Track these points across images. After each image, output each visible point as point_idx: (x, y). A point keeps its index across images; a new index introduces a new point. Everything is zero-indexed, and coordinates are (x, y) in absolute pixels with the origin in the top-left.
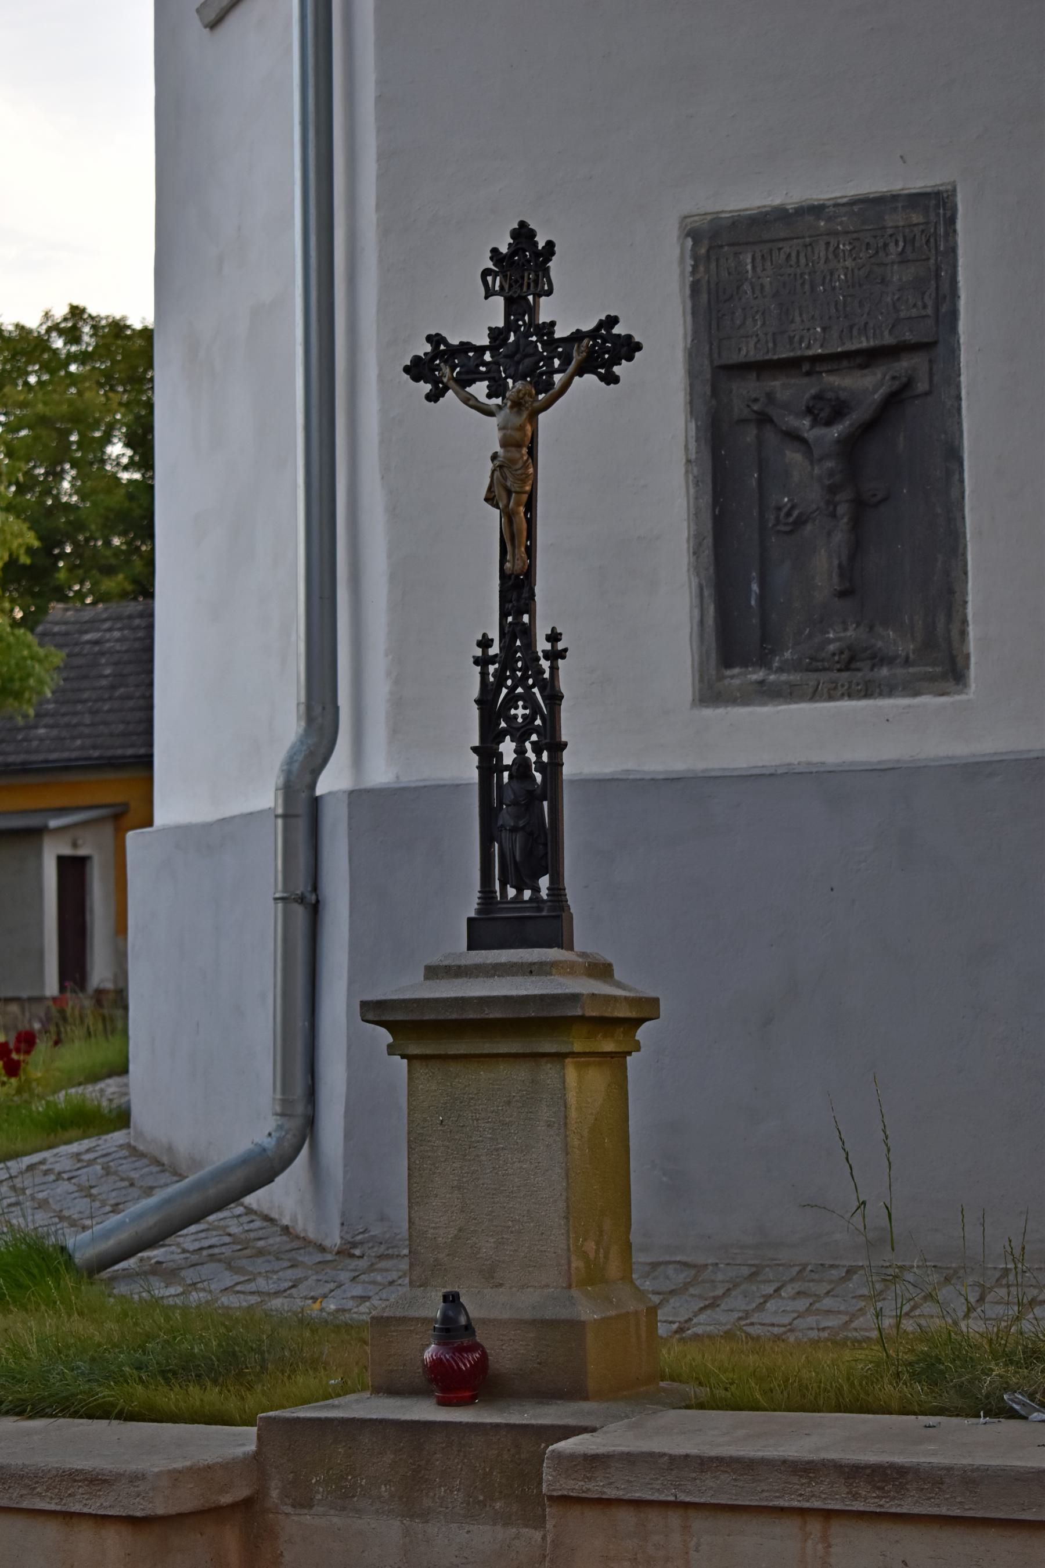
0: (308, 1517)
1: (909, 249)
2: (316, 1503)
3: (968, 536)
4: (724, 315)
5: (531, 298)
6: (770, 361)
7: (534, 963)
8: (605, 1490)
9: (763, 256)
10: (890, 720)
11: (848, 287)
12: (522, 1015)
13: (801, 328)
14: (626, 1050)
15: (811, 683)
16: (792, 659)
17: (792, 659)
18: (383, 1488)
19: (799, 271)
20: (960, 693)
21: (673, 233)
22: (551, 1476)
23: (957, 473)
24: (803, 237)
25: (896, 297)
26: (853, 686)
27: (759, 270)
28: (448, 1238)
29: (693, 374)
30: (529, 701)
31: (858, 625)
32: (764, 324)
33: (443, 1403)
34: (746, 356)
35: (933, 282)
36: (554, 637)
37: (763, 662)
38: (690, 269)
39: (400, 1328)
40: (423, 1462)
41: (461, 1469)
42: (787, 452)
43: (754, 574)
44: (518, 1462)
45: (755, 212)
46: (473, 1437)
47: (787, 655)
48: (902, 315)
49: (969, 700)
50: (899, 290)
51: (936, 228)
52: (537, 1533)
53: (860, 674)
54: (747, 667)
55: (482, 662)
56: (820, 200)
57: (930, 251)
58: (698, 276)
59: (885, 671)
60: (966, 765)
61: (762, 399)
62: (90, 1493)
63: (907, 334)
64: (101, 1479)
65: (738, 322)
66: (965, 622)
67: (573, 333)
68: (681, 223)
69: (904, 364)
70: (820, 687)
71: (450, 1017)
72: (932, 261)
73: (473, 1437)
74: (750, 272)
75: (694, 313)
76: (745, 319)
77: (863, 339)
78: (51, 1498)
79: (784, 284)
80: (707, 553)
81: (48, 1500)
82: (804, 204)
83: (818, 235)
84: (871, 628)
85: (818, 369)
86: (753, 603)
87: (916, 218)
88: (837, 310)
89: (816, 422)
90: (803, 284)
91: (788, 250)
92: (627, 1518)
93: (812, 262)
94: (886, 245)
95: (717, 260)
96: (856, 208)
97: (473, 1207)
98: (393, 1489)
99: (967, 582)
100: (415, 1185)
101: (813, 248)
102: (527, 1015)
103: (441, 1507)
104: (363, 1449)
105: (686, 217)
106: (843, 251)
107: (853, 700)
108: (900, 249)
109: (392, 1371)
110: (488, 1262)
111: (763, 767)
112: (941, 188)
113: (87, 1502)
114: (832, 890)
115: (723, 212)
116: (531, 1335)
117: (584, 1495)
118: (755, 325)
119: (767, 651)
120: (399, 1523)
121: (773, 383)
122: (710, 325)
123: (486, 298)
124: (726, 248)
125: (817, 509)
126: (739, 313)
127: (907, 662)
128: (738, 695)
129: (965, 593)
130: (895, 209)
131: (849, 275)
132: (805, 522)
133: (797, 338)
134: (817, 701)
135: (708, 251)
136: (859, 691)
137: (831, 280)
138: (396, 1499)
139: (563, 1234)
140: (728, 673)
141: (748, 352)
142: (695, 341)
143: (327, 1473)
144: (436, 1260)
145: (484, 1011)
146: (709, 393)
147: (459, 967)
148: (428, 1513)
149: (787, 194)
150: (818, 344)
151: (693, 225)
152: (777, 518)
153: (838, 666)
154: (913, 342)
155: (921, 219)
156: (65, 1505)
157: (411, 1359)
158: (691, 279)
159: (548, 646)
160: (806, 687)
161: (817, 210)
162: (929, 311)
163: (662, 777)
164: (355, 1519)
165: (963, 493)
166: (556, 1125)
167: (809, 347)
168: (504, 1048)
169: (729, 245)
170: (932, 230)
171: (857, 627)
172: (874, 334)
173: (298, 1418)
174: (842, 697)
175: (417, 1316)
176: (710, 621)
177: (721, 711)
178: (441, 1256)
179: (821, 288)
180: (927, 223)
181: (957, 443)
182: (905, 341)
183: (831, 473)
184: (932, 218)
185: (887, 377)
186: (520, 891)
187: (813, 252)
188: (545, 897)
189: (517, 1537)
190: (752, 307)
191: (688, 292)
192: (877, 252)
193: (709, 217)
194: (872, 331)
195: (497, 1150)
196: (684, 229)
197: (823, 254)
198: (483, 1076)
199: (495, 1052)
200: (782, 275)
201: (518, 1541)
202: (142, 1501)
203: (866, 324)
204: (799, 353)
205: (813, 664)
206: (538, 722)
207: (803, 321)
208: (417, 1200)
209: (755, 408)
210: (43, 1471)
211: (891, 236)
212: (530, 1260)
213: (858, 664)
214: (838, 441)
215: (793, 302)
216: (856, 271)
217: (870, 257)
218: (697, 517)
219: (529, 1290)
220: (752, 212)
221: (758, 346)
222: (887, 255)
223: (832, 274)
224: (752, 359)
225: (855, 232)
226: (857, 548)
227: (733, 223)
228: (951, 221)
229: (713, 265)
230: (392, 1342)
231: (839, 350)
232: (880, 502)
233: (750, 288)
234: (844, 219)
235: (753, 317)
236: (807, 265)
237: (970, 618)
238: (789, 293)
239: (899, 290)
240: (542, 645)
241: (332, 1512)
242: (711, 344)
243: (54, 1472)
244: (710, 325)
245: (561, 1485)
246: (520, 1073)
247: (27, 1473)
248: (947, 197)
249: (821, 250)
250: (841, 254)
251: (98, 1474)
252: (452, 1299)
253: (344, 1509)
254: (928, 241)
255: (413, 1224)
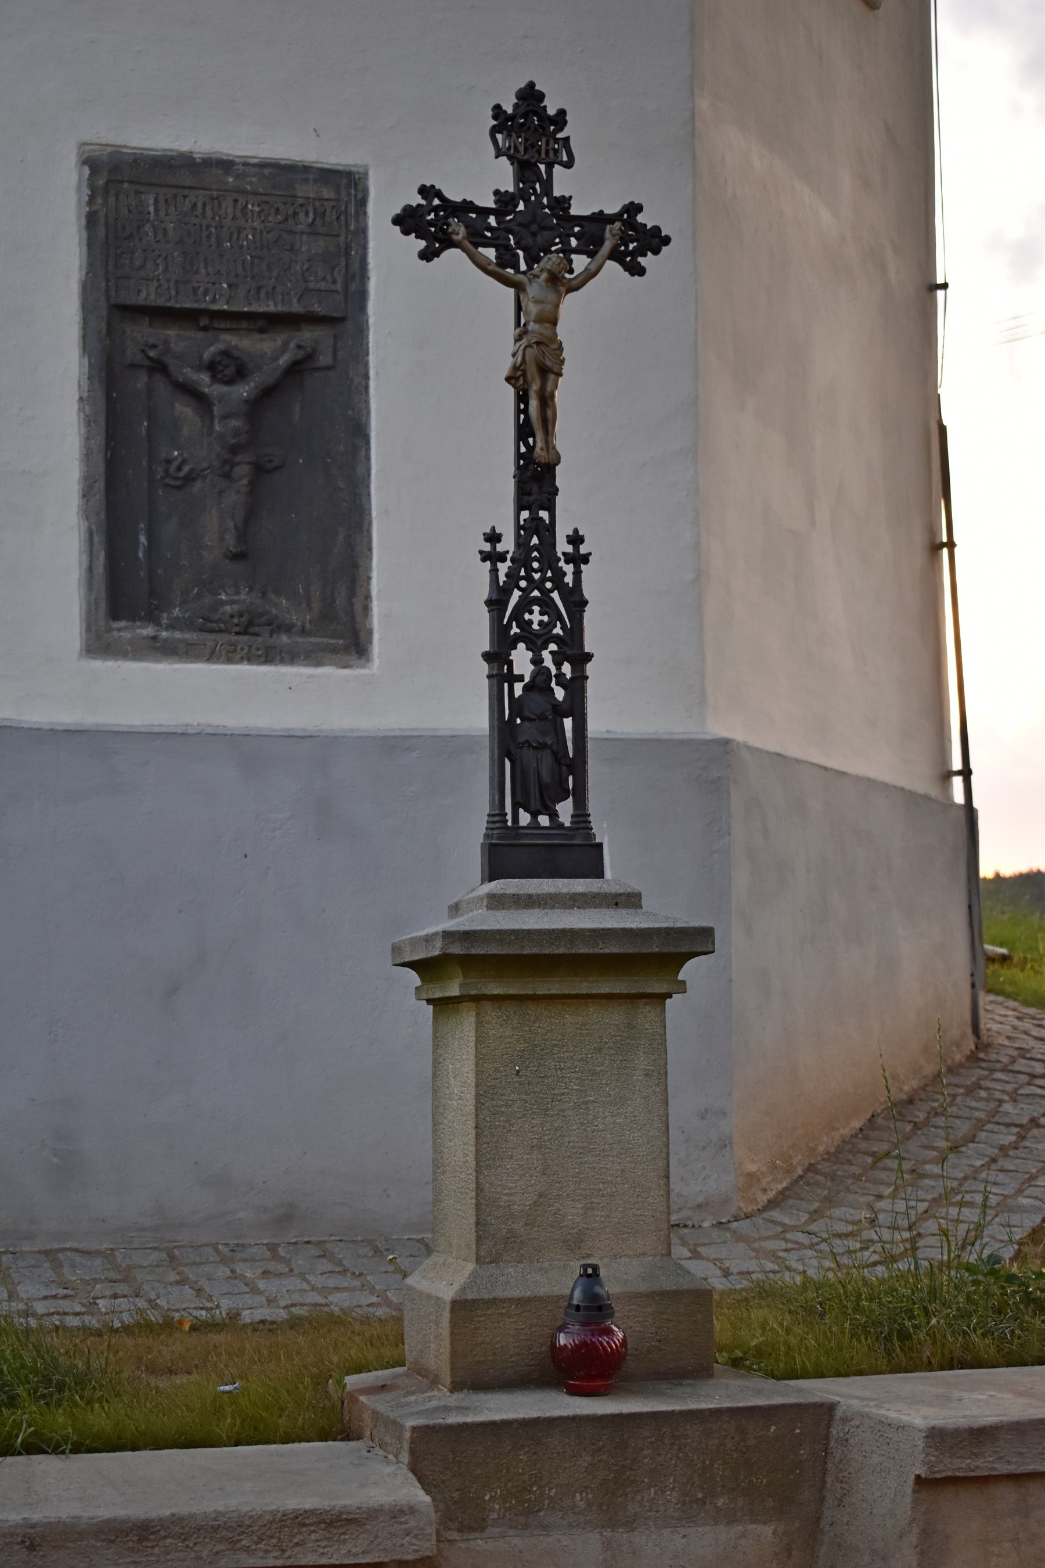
0: (480, 1541)
1: (319, 222)
2: (490, 1522)
3: (374, 514)
4: (122, 253)
5: (542, 167)
6: (170, 308)
7: (621, 895)
8: (995, 1466)
9: (166, 200)
10: (293, 687)
11: (256, 248)
12: (644, 951)
13: (207, 280)
14: (663, 990)
15: (209, 644)
16: (184, 617)
17: (184, 617)
18: (578, 1497)
19: (204, 223)
20: (363, 667)
21: (72, 159)
22: (934, 1456)
23: (363, 449)
24: (210, 190)
25: (305, 267)
26: (253, 650)
27: (162, 213)
28: (525, 1206)
29: (87, 309)
30: (547, 604)
31: (251, 589)
32: (166, 270)
33: (575, 1391)
34: (145, 299)
35: (343, 259)
36: (576, 539)
37: (152, 618)
38: (87, 198)
39: (489, 1312)
40: (628, 1462)
41: (676, 1465)
42: (177, 405)
43: (142, 525)
44: (744, 1450)
45: (160, 153)
46: (688, 1427)
47: (176, 613)
48: (312, 285)
49: (373, 675)
50: (308, 261)
51: (346, 207)
52: (767, 1529)
53: (260, 639)
54: (134, 620)
55: (493, 557)
56: (230, 155)
57: (340, 228)
58: (94, 208)
59: (285, 639)
60: (385, 738)
61: (161, 347)
62: (328, 1539)
63: (316, 305)
64: (346, 1519)
65: (138, 263)
66: (368, 597)
67: (594, 213)
68: (79, 148)
69: (307, 335)
70: (218, 648)
71: (556, 952)
72: (342, 239)
73: (688, 1427)
74: (152, 214)
75: (90, 245)
76: (146, 259)
77: (271, 303)
78: (267, 1551)
79: (189, 234)
80: (98, 498)
81: (261, 1554)
82: (212, 156)
83: (226, 191)
84: (264, 594)
85: (216, 326)
86: (141, 555)
87: (327, 193)
88: (244, 270)
89: (214, 378)
90: (209, 236)
91: (194, 200)
92: (1007, 1495)
93: (220, 216)
94: (295, 214)
95: (117, 195)
96: (266, 171)
97: (556, 1168)
98: (590, 1496)
99: (371, 559)
100: (484, 1146)
101: (219, 201)
102: (650, 950)
103: (650, 1511)
104: (552, 1453)
105: (85, 144)
106: (252, 211)
107: (253, 664)
108: (310, 220)
109: (479, 1362)
110: (576, 1231)
111: (160, 725)
112: (353, 169)
113: (326, 1550)
114: (246, 856)
115: (125, 147)
116: (649, 1310)
117: (972, 1474)
118: (157, 269)
119: (153, 606)
120: (598, 1536)
121: (168, 332)
122: (107, 261)
123: (497, 157)
124: (126, 185)
125: (209, 468)
126: (139, 253)
127: (303, 632)
128: (129, 648)
129: (368, 569)
130: (306, 180)
131: (258, 237)
132: (194, 479)
133: (201, 290)
134: (215, 663)
135: (107, 183)
136: (259, 656)
137: (238, 238)
138: (594, 1508)
139: (662, 1196)
140: (116, 625)
141: (148, 295)
142: (90, 275)
143: (506, 1485)
144: (510, 1231)
145: (598, 945)
146: (104, 331)
147: (530, 896)
148: (634, 1520)
149: (195, 142)
150: (224, 300)
151: (91, 154)
152: (166, 472)
153: (237, 629)
154: (321, 314)
155: (332, 195)
156: (290, 1557)
157: (502, 1347)
158: (87, 209)
159: (569, 549)
160: (203, 647)
161: (226, 165)
162: (339, 287)
163: (61, 728)
164: (541, 1538)
165: (369, 470)
166: (655, 1074)
167: (214, 301)
168: (605, 987)
169: (129, 182)
170: (343, 208)
171: (249, 592)
172: (283, 299)
173: (465, 1424)
174: (241, 660)
175: (510, 1296)
176: (100, 569)
177: (110, 664)
178: (515, 1226)
179: (228, 244)
180: (338, 200)
181: (364, 419)
182: (313, 312)
183: (237, 433)
184: (343, 196)
185: (292, 345)
186: (534, 815)
187: (220, 206)
188: (568, 824)
189: (743, 1535)
190: (153, 251)
191: (83, 222)
192: (286, 219)
193: (109, 149)
194: (280, 296)
195: (586, 1103)
196: (81, 156)
197: (230, 210)
198: (570, 1019)
199: (594, 992)
200: (186, 224)
201: (744, 1540)
202: (414, 1541)
203: (274, 288)
204: (203, 306)
205: (209, 624)
206: (558, 630)
207: (208, 274)
208: (487, 1163)
209: (152, 354)
210: (251, 1517)
211: (301, 205)
212: (625, 1227)
213: (256, 629)
214: (246, 401)
215: (198, 253)
216: (265, 233)
217: (279, 223)
218: (88, 458)
219: (622, 1259)
220: (156, 153)
221: (159, 291)
222: (296, 224)
223: (239, 233)
224: (153, 304)
225: (264, 195)
226: (251, 514)
227: (135, 161)
228: (363, 202)
229: (112, 200)
230: (479, 1328)
231: (246, 309)
232: (276, 469)
233: (152, 229)
234: (253, 179)
235: (155, 261)
236: (213, 218)
237: (374, 593)
238: (195, 242)
239: (308, 261)
240: (563, 547)
241: (511, 1532)
242: (108, 281)
243: (268, 1517)
244: (107, 261)
245: (945, 1465)
246: (614, 1017)
247: (225, 1523)
248: (359, 179)
249: (227, 205)
250: (250, 214)
251: (341, 1513)
252: (591, 1275)
253: (526, 1526)
254: (338, 218)
255: (482, 1191)
